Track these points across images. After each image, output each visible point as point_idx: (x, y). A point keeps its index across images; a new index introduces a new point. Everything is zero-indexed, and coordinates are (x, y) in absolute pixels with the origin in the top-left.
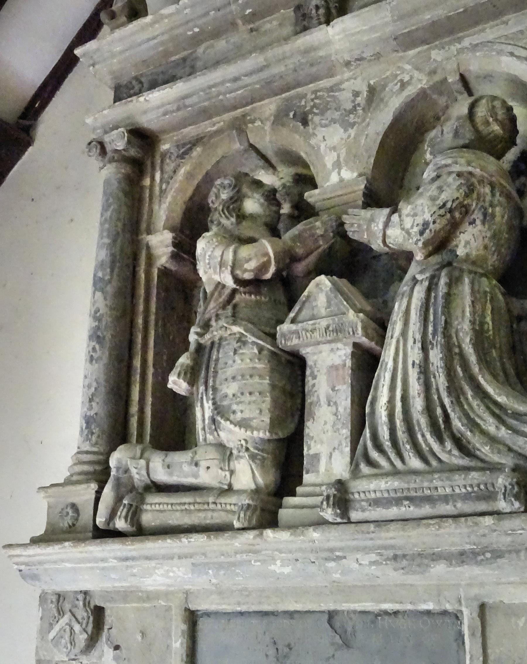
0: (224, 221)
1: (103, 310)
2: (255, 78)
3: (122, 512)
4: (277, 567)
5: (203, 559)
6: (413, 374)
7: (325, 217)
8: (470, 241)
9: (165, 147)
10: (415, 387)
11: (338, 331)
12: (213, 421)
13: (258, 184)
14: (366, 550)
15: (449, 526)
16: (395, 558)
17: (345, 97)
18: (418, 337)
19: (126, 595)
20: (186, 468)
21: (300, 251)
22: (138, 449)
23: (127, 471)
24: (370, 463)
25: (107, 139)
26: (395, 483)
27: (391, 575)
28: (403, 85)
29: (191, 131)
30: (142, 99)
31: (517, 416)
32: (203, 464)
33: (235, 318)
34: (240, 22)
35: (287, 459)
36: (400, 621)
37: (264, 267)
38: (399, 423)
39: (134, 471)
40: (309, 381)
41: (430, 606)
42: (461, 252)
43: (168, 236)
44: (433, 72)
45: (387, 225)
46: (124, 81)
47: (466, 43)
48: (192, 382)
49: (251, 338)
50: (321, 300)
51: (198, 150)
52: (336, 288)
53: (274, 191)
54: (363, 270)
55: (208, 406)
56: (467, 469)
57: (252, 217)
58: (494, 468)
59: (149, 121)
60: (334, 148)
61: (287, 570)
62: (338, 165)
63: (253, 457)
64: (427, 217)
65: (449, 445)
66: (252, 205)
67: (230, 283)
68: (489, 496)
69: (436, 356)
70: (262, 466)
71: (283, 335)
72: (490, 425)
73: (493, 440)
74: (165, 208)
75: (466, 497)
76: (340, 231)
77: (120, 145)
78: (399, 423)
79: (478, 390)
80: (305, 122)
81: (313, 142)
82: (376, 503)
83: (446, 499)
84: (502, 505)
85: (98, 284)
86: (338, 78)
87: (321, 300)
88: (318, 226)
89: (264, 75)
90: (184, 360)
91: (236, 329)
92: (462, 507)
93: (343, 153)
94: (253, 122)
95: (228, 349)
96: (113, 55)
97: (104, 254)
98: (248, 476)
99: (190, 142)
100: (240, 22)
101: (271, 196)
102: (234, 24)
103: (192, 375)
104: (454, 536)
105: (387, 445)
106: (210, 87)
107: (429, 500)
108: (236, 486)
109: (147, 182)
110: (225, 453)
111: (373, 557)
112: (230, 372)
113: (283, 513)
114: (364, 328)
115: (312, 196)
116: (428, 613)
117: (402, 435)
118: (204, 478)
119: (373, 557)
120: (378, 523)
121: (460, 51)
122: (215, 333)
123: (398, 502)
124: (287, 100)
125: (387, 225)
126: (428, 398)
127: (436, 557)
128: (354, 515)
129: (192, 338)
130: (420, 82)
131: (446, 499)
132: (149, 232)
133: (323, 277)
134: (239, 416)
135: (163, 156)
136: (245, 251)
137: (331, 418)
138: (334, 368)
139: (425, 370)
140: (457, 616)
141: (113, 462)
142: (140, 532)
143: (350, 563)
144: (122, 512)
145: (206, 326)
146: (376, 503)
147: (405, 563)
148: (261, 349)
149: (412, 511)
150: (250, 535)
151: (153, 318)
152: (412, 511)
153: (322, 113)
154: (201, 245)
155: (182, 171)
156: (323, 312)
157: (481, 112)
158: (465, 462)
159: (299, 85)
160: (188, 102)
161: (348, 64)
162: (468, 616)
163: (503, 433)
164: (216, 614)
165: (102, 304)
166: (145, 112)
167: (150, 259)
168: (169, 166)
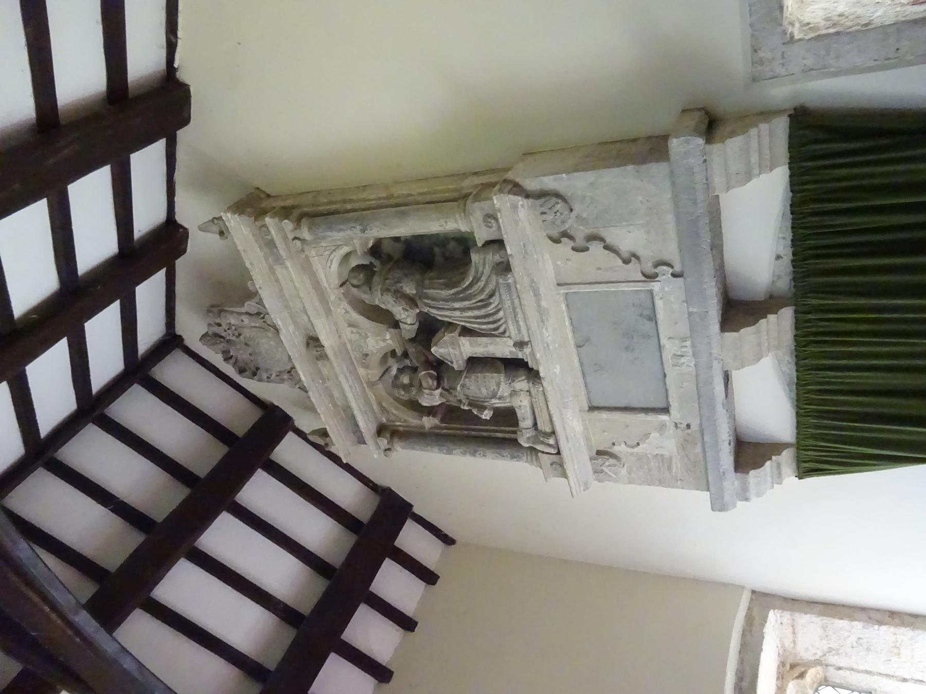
0: (414, 393)
1: (461, 450)
2: (350, 379)
3: (546, 441)
4: (558, 370)
7: (407, 347)
8: (409, 289)
9: (384, 420)
10: (470, 314)
11: (454, 344)
12: (500, 399)
13: (396, 377)
14: (542, 334)
15: (524, 302)
16: (543, 321)
17: (354, 337)
19: (587, 439)
21: (423, 359)
22: (519, 433)
23: (528, 438)
24: (504, 332)
25: (383, 448)
26: (510, 323)
28: (347, 312)
29: (375, 407)
32: (519, 403)
33: (455, 389)
37: (431, 376)
39: (528, 435)
41: (564, 307)
42: (414, 292)
43: (425, 419)
44: (340, 299)
45: (406, 323)
47: (326, 285)
48: (485, 408)
49: (462, 382)
50: (441, 350)
51: (384, 404)
52: (436, 345)
53: (398, 369)
55: (494, 401)
57: (411, 379)
58: (497, 283)
59: (373, 428)
60: (377, 342)
61: (558, 367)
63: (513, 381)
64: (400, 308)
65: (491, 301)
66: (405, 380)
67: (439, 391)
70: (517, 377)
72: (481, 284)
74: (412, 420)
76: (412, 340)
77: (386, 441)
79: (471, 285)
82: (519, 330)
85: (449, 452)
86: (347, 341)
87: (441, 350)
88: (411, 350)
89: (348, 375)
90: (475, 412)
91: (459, 388)
92: (515, 296)
95: (467, 392)
97: (436, 449)
98: (522, 384)
101: (400, 371)
103: (482, 408)
104: (528, 299)
107: (514, 309)
108: (527, 389)
109: (401, 429)
110: (514, 393)
111: (544, 331)
112: (478, 392)
114: (451, 332)
115: (399, 352)
116: (567, 306)
119: (544, 331)
120: (528, 330)
122: (462, 397)
123: (517, 322)
125: (406, 323)
127: (539, 306)
128: (526, 339)
129: (466, 408)
130: (345, 305)
131: (513, 303)
132: (424, 427)
134: (495, 387)
135: (388, 420)
136: (424, 384)
141: (527, 445)
144: (546, 441)
145: (460, 401)
147: (544, 318)
148: (466, 377)
149: (520, 316)
150: (544, 383)
151: (464, 426)
154: (425, 404)
157: (355, 282)
158: (497, 294)
159: (351, 358)
161: (340, 337)
162: (563, 290)
165: (458, 451)
167: (436, 427)
168: (392, 418)
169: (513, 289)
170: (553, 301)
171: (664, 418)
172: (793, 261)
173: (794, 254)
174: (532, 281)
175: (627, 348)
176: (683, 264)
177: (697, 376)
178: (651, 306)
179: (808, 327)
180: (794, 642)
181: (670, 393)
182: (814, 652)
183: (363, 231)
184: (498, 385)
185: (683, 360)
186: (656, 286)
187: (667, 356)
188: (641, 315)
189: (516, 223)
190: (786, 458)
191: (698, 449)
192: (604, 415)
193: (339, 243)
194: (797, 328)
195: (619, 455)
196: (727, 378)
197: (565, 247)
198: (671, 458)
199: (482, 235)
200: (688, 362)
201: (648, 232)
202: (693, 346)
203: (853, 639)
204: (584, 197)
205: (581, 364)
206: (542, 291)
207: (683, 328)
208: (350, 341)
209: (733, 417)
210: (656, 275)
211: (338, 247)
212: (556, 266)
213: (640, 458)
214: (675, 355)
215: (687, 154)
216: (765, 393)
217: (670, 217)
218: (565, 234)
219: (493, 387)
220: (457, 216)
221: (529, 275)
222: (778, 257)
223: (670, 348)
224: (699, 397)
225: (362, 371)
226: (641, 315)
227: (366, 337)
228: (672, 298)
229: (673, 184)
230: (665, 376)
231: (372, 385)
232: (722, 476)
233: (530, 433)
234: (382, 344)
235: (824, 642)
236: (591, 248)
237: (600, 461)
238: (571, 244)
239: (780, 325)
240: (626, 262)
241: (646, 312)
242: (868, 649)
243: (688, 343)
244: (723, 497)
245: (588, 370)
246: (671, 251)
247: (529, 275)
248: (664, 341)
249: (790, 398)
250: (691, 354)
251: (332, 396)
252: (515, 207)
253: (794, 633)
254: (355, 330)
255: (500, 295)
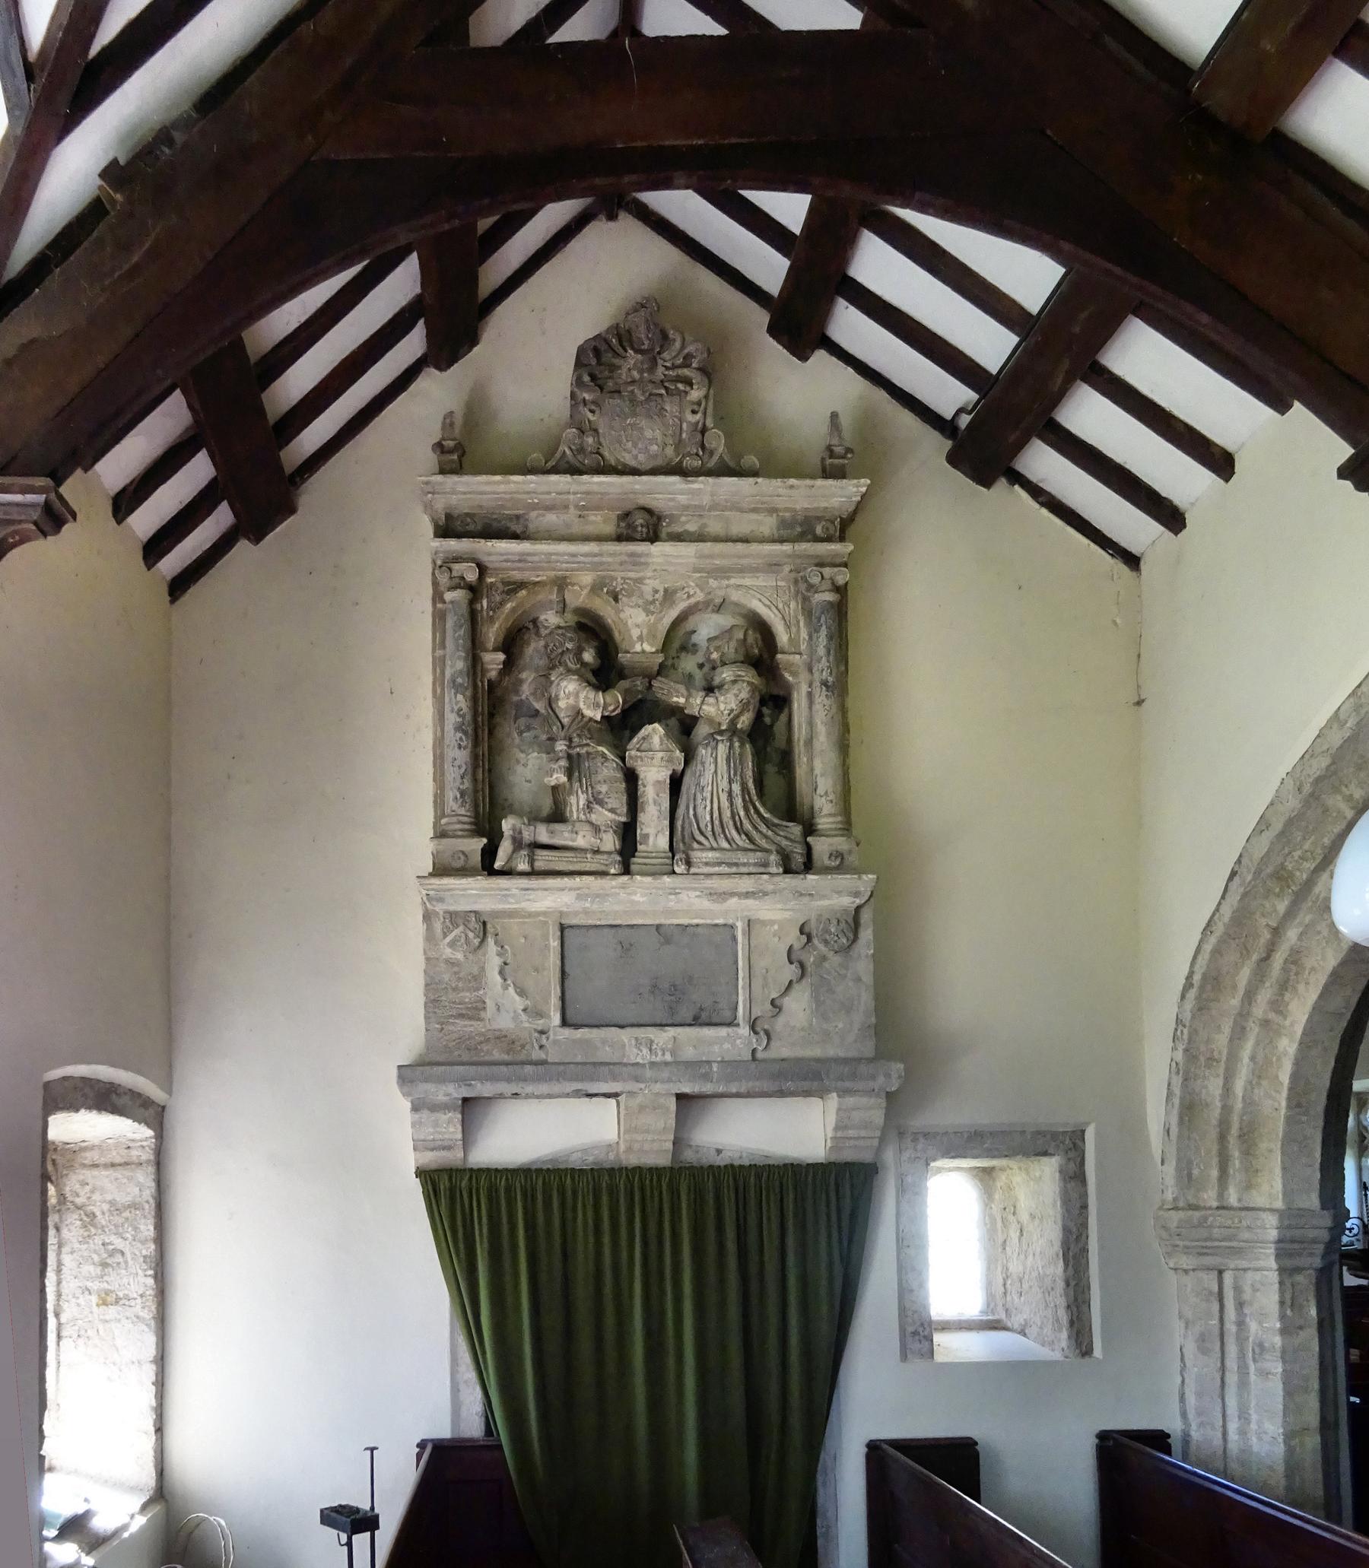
4: (638, 898)
5: (586, 891)
6: (724, 797)
10: (725, 804)
14: (695, 889)
18: (726, 776)
19: (511, 914)
20: (566, 835)
23: (520, 833)
26: (717, 854)
27: (706, 904)
28: (689, 597)
30: (489, 544)
31: (776, 825)
34: (572, 508)
35: (628, 834)
36: (699, 929)
38: (717, 822)
40: (641, 789)
41: (721, 921)
46: (456, 513)
47: (732, 581)
50: (656, 741)
54: (684, 727)
56: (746, 850)
60: (638, 626)
62: (641, 638)
68: (766, 865)
69: (736, 788)
71: (631, 757)
72: (763, 828)
73: (766, 837)
75: (755, 864)
78: (717, 822)
80: (616, 600)
81: (622, 615)
82: (707, 864)
83: (744, 865)
84: (774, 870)
87: (656, 741)
93: (645, 632)
94: (573, 585)
96: (454, 492)
99: (515, 583)
100: (572, 508)
102: (566, 507)
104: (746, 884)
105: (709, 834)
106: (551, 554)
107: (736, 865)
110: (596, 829)
113: (633, 867)
116: (716, 925)
117: (718, 829)
118: (580, 841)
120: (709, 875)
121: (728, 586)
123: (719, 864)
124: (604, 577)
125: (703, 703)
126: (732, 812)
127: (732, 894)
128: (693, 870)
130: (700, 596)
131: (744, 865)
133: (656, 725)
137: (656, 813)
138: (658, 782)
139: (730, 793)
140: (732, 927)
142: (533, 873)
143: (683, 896)
146: (707, 864)
149: (727, 870)
152: (727, 870)
153: (629, 596)
155: (509, 605)
156: (657, 747)
158: (751, 847)
160: (529, 558)
163: (770, 833)
164: (578, 927)
166: (490, 554)
169: (762, 870)
170: (734, 911)
171: (556, 1019)
172: (732, 1166)
173: (741, 1167)
174: (766, 894)
175: (655, 986)
176: (764, 1061)
177: (625, 1065)
178: (715, 1020)
179: (651, 1180)
180: (95, 1166)
181: (595, 1031)
182: (82, 1193)
183: (824, 683)
184: (612, 811)
185: (645, 1051)
186: (744, 1030)
187: (651, 1033)
188: (701, 1009)
189: (839, 893)
190: (454, 1157)
191: (497, 1055)
192: (555, 944)
193: (794, 629)
194: (650, 1169)
195: (480, 952)
196: (615, 1095)
197: (793, 938)
198: (479, 1019)
199: (821, 847)
200: (643, 1056)
201: (803, 1029)
202: (666, 1064)
203: (119, 1243)
204: (847, 969)
205: (632, 926)
206: (750, 902)
207: (689, 1053)
208: (640, 581)
209: (501, 1096)
210: (756, 1033)
211: (788, 627)
212: (772, 922)
213: (477, 980)
214: (652, 1042)
215: (888, 1076)
216: (531, 1132)
217: (816, 1052)
218: (809, 938)
219: (612, 803)
220: (839, 819)
221: (774, 892)
222: (719, 1151)
223: (663, 1037)
224: (594, 1064)
225: (587, 579)
226: (701, 1009)
227: (648, 612)
228: (726, 1046)
229: (859, 1060)
230: (622, 1027)
231: (561, 584)
232: (464, 1081)
233: (527, 836)
234: (635, 633)
235: (106, 1207)
236: (793, 967)
237: (473, 924)
238: (797, 946)
239: (653, 1149)
240: (773, 1002)
241: (704, 1016)
242: (104, 1265)
243: (668, 1057)
244: (426, 1080)
245: (625, 936)
246: (781, 1050)
247: (774, 892)
248: (671, 1032)
249: (534, 1162)
250: (654, 1058)
251: (550, 508)
252: (857, 894)
253: (113, 1165)
254: (660, 596)
255: (746, 850)
